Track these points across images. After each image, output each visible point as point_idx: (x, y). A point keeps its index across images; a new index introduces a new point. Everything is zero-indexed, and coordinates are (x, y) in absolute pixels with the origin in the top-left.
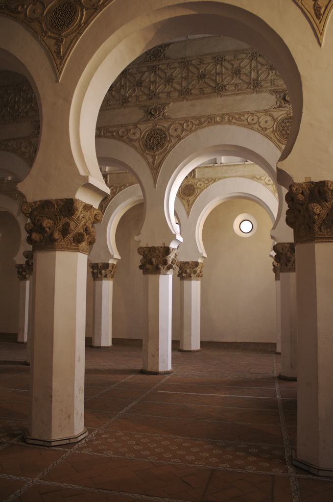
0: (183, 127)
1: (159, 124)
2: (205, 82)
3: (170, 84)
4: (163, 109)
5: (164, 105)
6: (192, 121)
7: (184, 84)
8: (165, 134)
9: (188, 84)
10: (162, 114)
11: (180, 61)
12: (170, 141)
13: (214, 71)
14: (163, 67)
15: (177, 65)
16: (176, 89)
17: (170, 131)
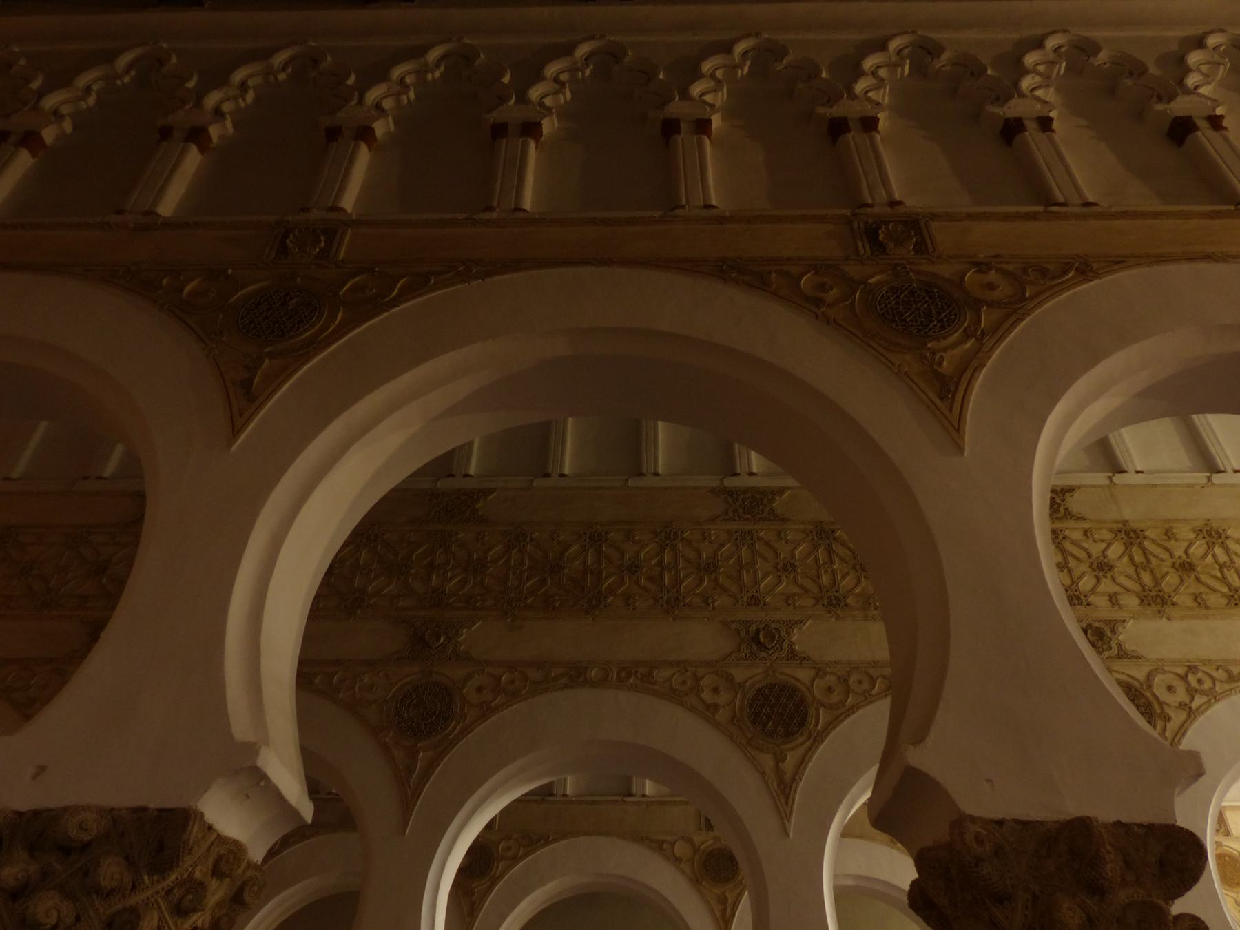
0: (1188, 684)
1: (1115, 668)
2: (1198, 579)
3: (1109, 575)
4: (1114, 632)
5: (1113, 625)
6: (1206, 669)
7: (1147, 578)
8: (1143, 696)
9: (1157, 582)
10: (1113, 644)
11: (1116, 526)
12: (1167, 719)
13: (1209, 559)
14: (1077, 535)
15: (1108, 536)
16: (1128, 590)
17: (1155, 690)
